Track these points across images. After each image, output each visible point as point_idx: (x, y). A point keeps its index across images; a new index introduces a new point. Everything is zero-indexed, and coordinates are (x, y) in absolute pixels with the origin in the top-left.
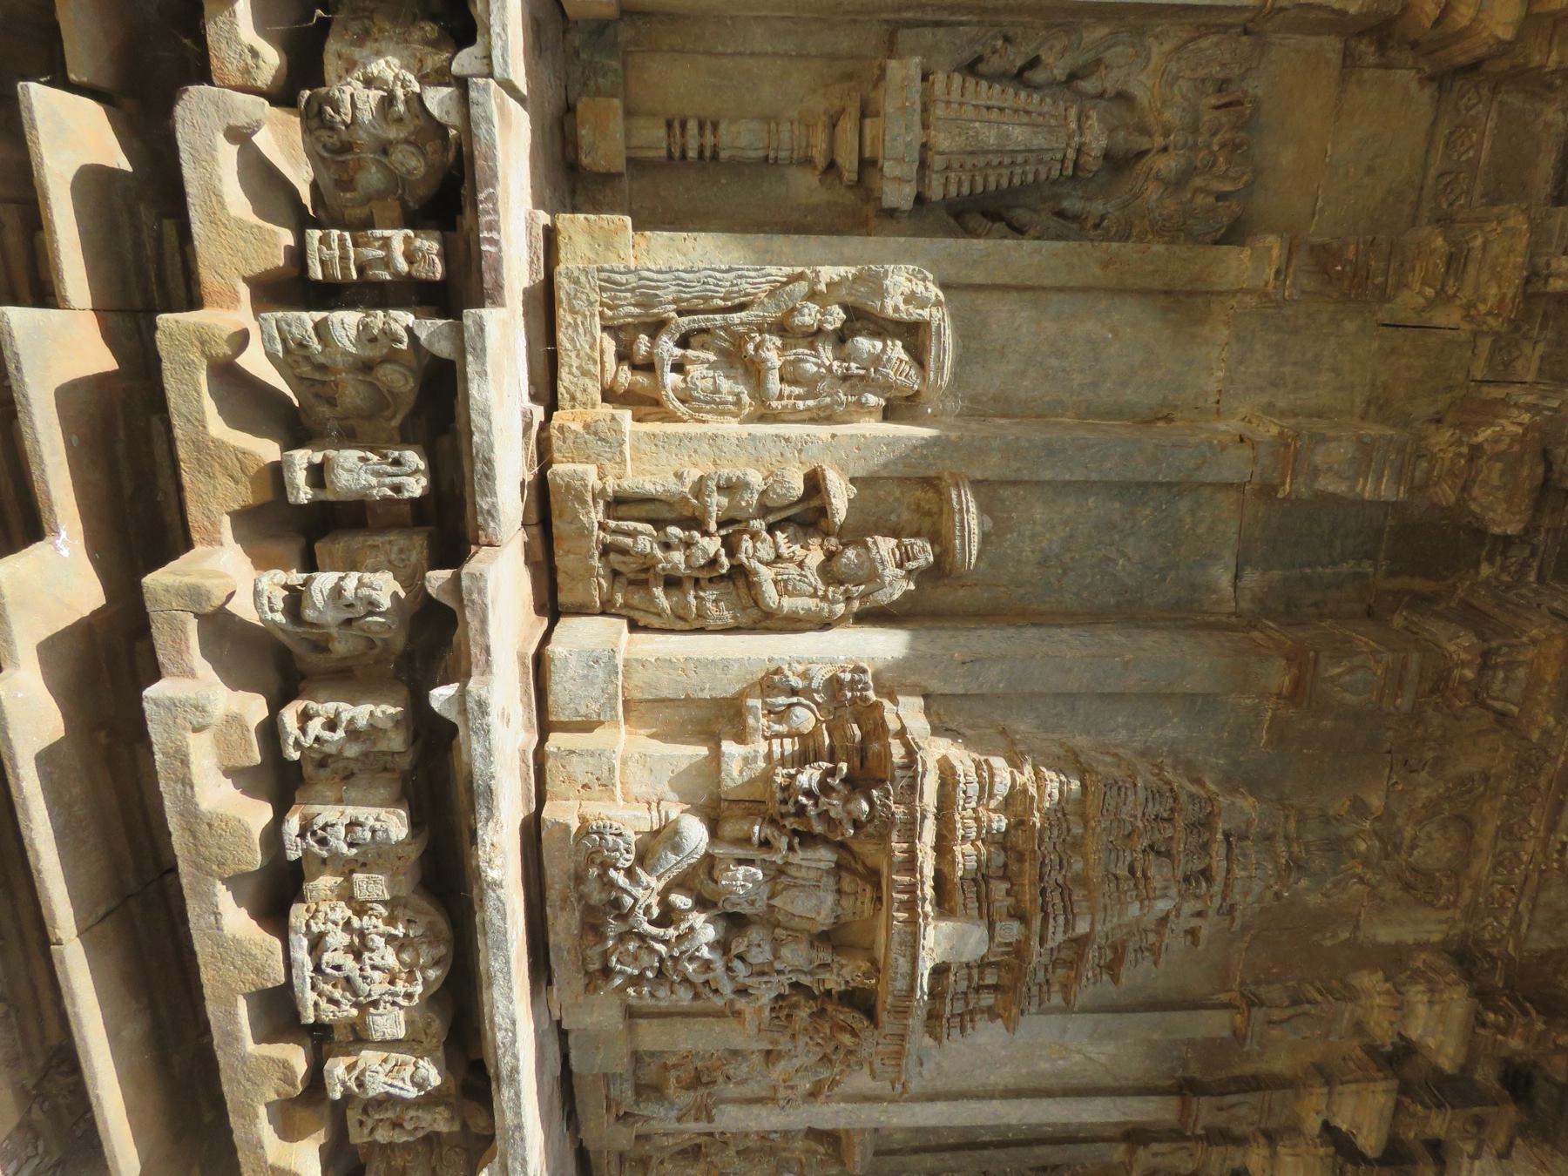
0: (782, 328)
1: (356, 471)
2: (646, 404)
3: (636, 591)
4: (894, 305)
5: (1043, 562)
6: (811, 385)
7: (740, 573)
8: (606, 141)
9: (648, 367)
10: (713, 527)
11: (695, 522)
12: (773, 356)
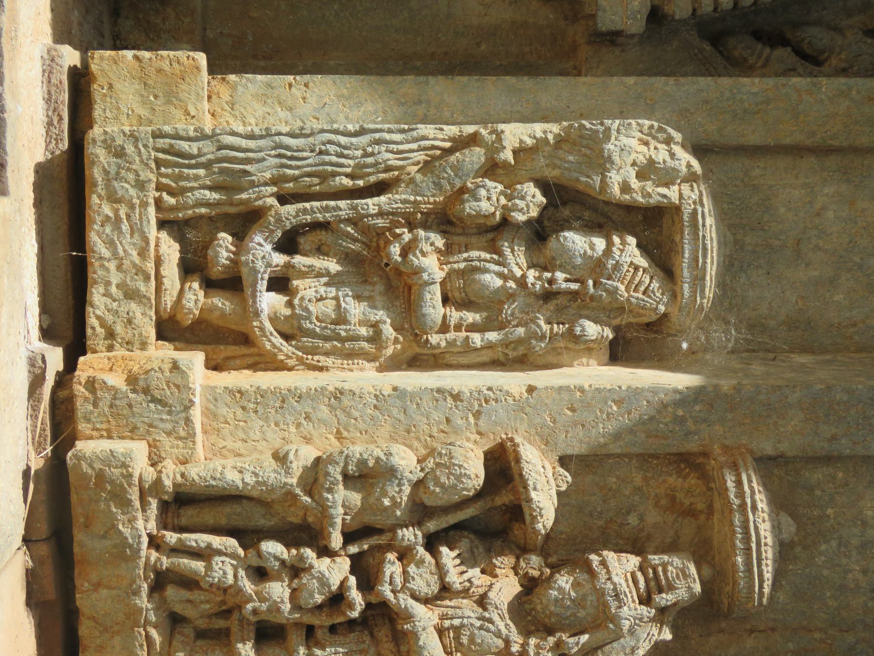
0: (445, 220)
2: (227, 342)
4: (621, 180)
6: (492, 308)
9: (232, 283)
10: (336, 540)
11: (307, 533)
12: (431, 265)
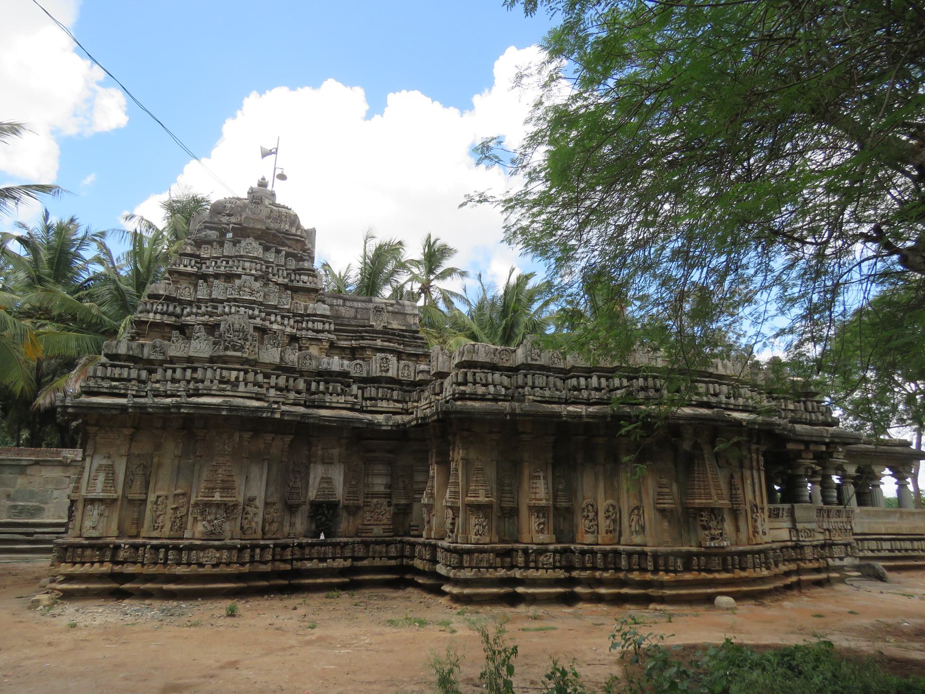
1: (161, 556)
2: (162, 527)
3: (182, 528)
4: (154, 500)
8: (134, 531)
12: (158, 513)
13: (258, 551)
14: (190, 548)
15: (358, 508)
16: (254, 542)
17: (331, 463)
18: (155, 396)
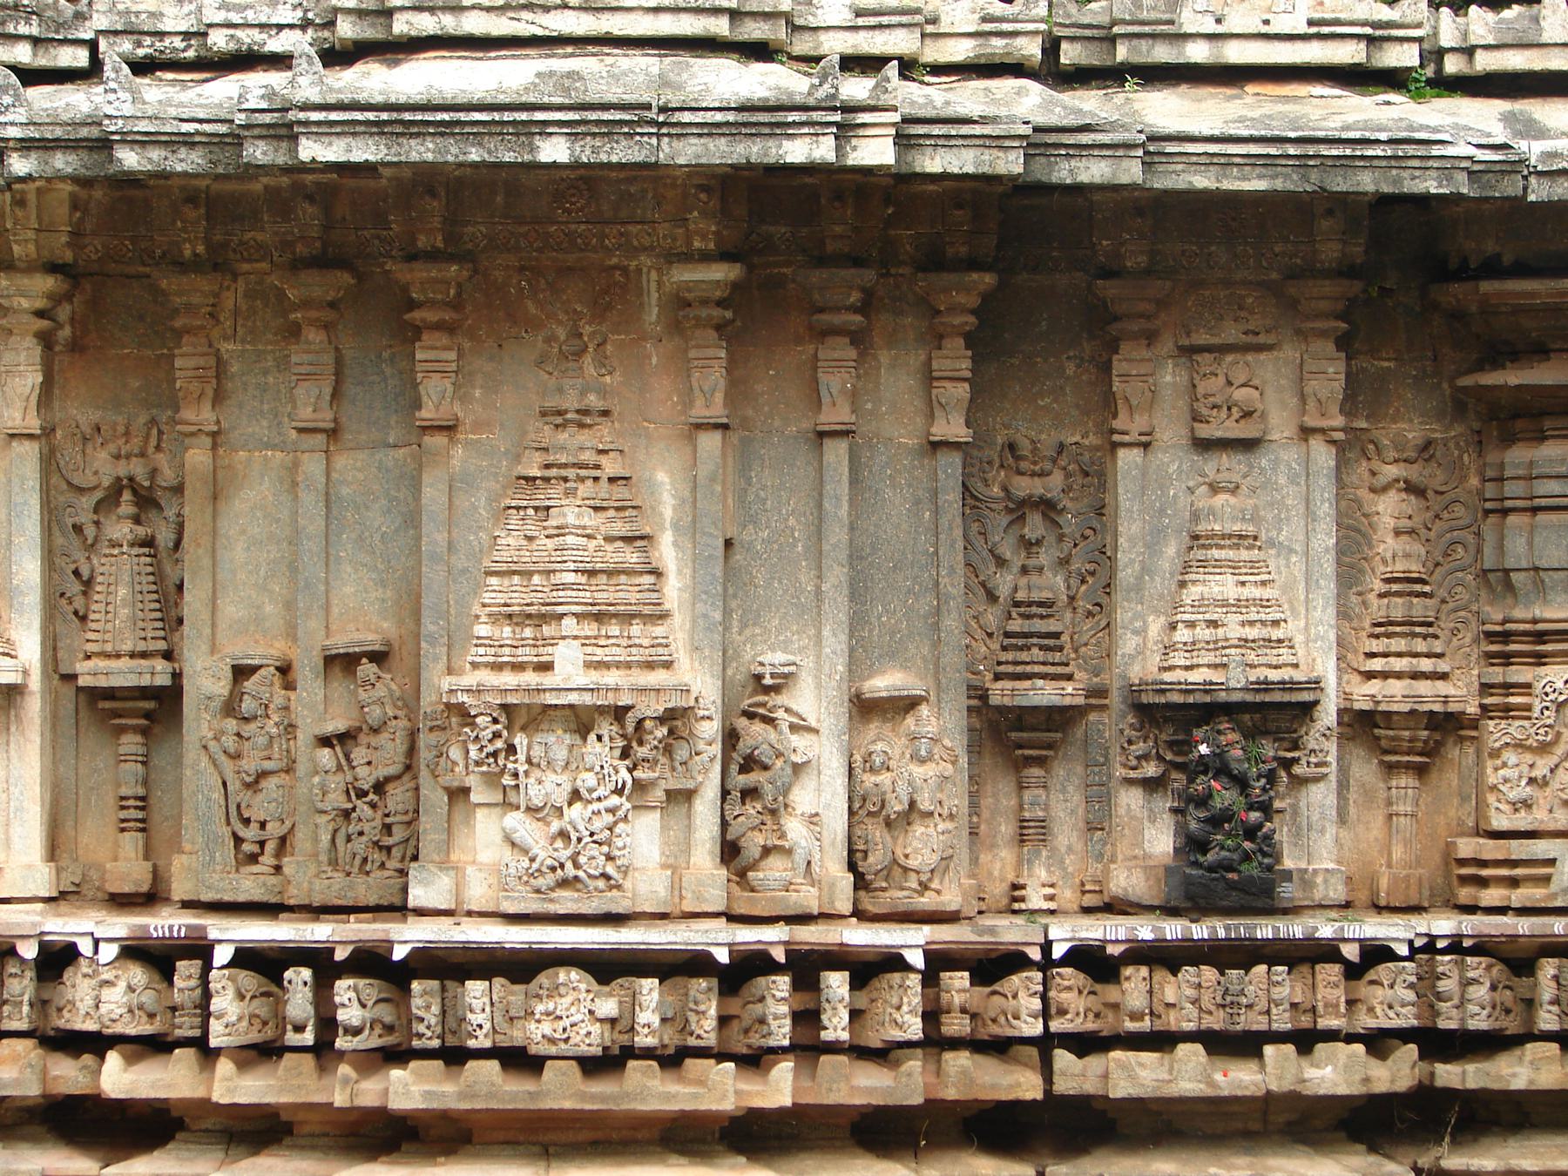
0: (236, 756)
5: (383, 583)
7: (379, 787)
8: (131, 872)
10: (350, 806)
12: (251, 764)
13: (836, 983)
14: (452, 966)
15: (1447, 726)
16: (811, 935)
17: (1248, 445)
18: (142, 67)
